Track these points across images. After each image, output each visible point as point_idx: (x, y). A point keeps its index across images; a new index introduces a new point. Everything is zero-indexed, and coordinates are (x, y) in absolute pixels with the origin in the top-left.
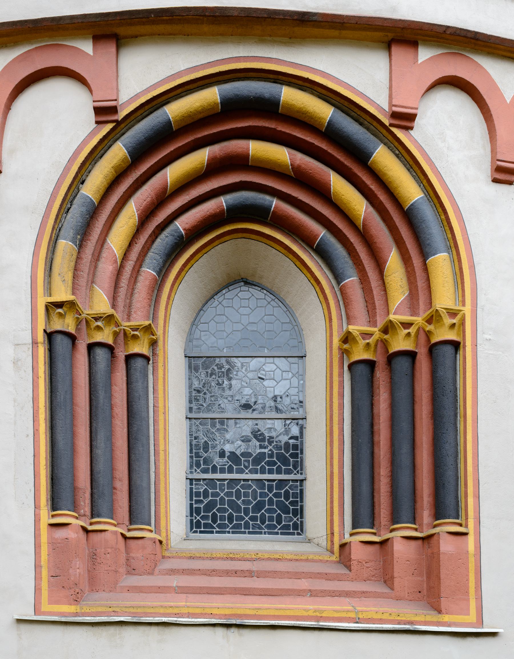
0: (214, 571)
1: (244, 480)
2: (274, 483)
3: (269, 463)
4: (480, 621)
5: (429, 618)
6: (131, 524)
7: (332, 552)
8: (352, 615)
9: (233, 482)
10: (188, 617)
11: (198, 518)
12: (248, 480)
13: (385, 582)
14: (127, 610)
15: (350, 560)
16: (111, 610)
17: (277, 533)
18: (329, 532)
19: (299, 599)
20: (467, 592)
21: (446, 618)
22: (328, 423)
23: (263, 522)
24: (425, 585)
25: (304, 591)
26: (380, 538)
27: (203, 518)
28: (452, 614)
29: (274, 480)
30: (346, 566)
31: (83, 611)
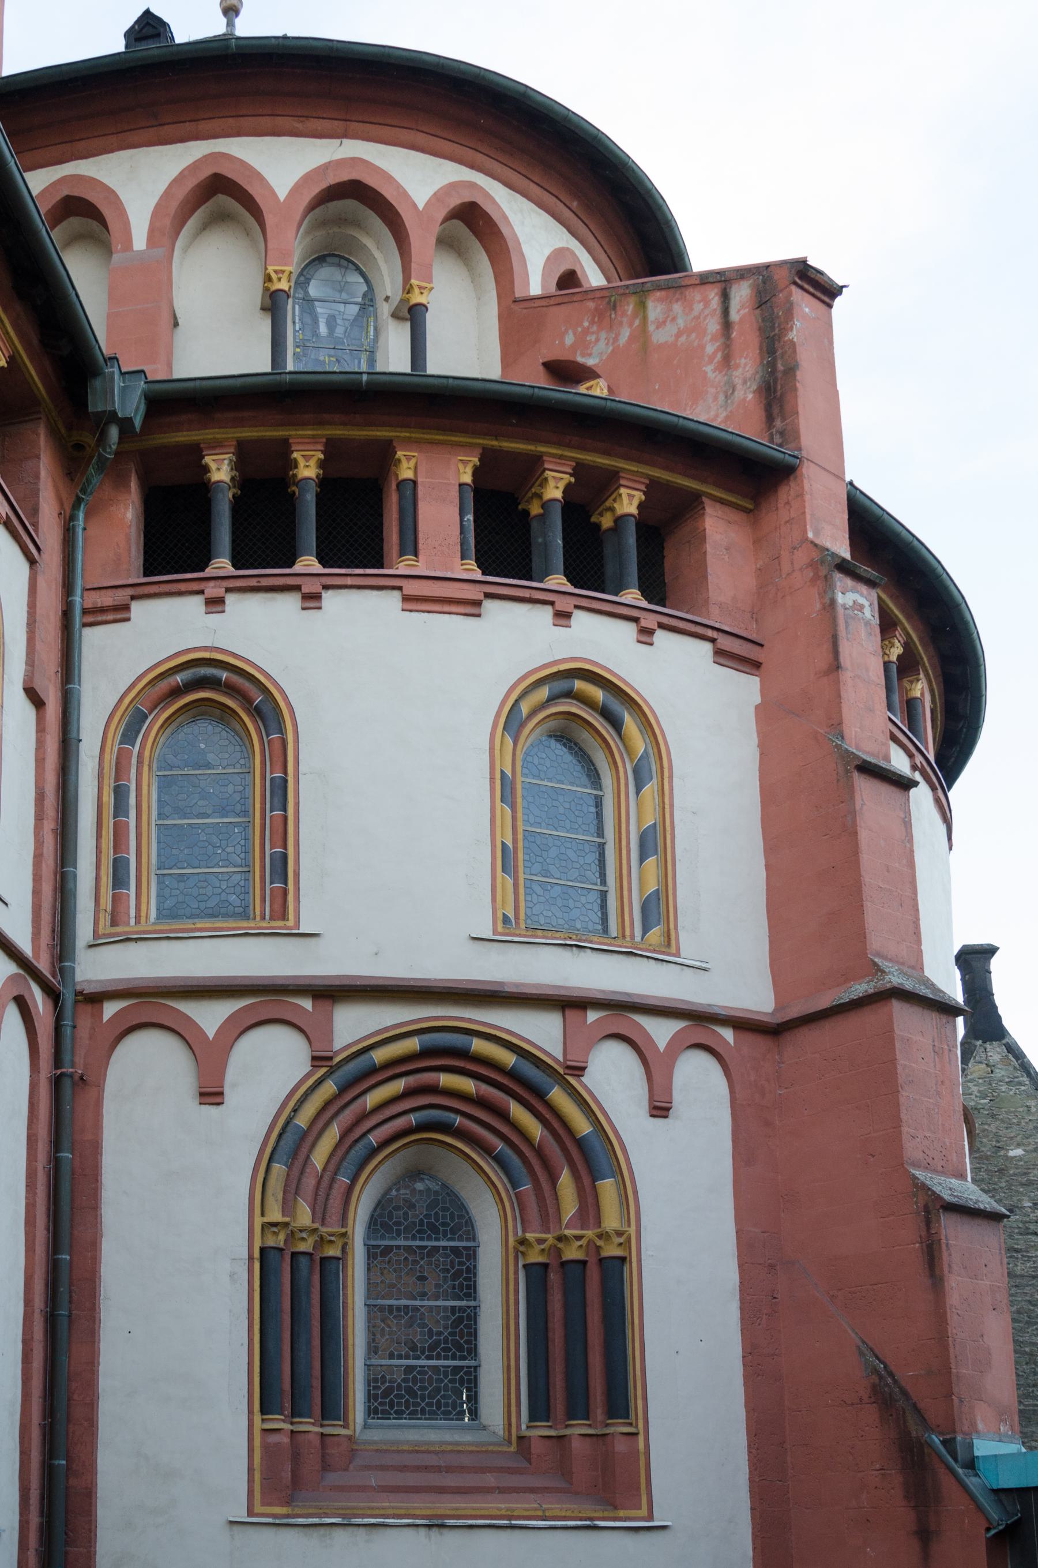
0: (405, 1466)
1: (420, 1366)
2: (449, 1369)
3: (444, 1350)
4: (650, 1517)
5: (606, 1514)
6: (323, 1419)
7: (510, 1442)
8: (540, 1513)
10: (393, 1518)
11: (376, 1404)
12: (424, 1367)
13: (563, 1475)
14: (337, 1512)
15: (530, 1453)
16: (321, 1511)
17: (452, 1419)
18: (506, 1423)
20: (639, 1488)
21: (621, 1513)
22: (505, 1317)
23: (439, 1407)
24: (600, 1479)
26: (557, 1432)
27: (381, 1404)
28: (626, 1509)
30: (525, 1458)
31: (294, 1512)
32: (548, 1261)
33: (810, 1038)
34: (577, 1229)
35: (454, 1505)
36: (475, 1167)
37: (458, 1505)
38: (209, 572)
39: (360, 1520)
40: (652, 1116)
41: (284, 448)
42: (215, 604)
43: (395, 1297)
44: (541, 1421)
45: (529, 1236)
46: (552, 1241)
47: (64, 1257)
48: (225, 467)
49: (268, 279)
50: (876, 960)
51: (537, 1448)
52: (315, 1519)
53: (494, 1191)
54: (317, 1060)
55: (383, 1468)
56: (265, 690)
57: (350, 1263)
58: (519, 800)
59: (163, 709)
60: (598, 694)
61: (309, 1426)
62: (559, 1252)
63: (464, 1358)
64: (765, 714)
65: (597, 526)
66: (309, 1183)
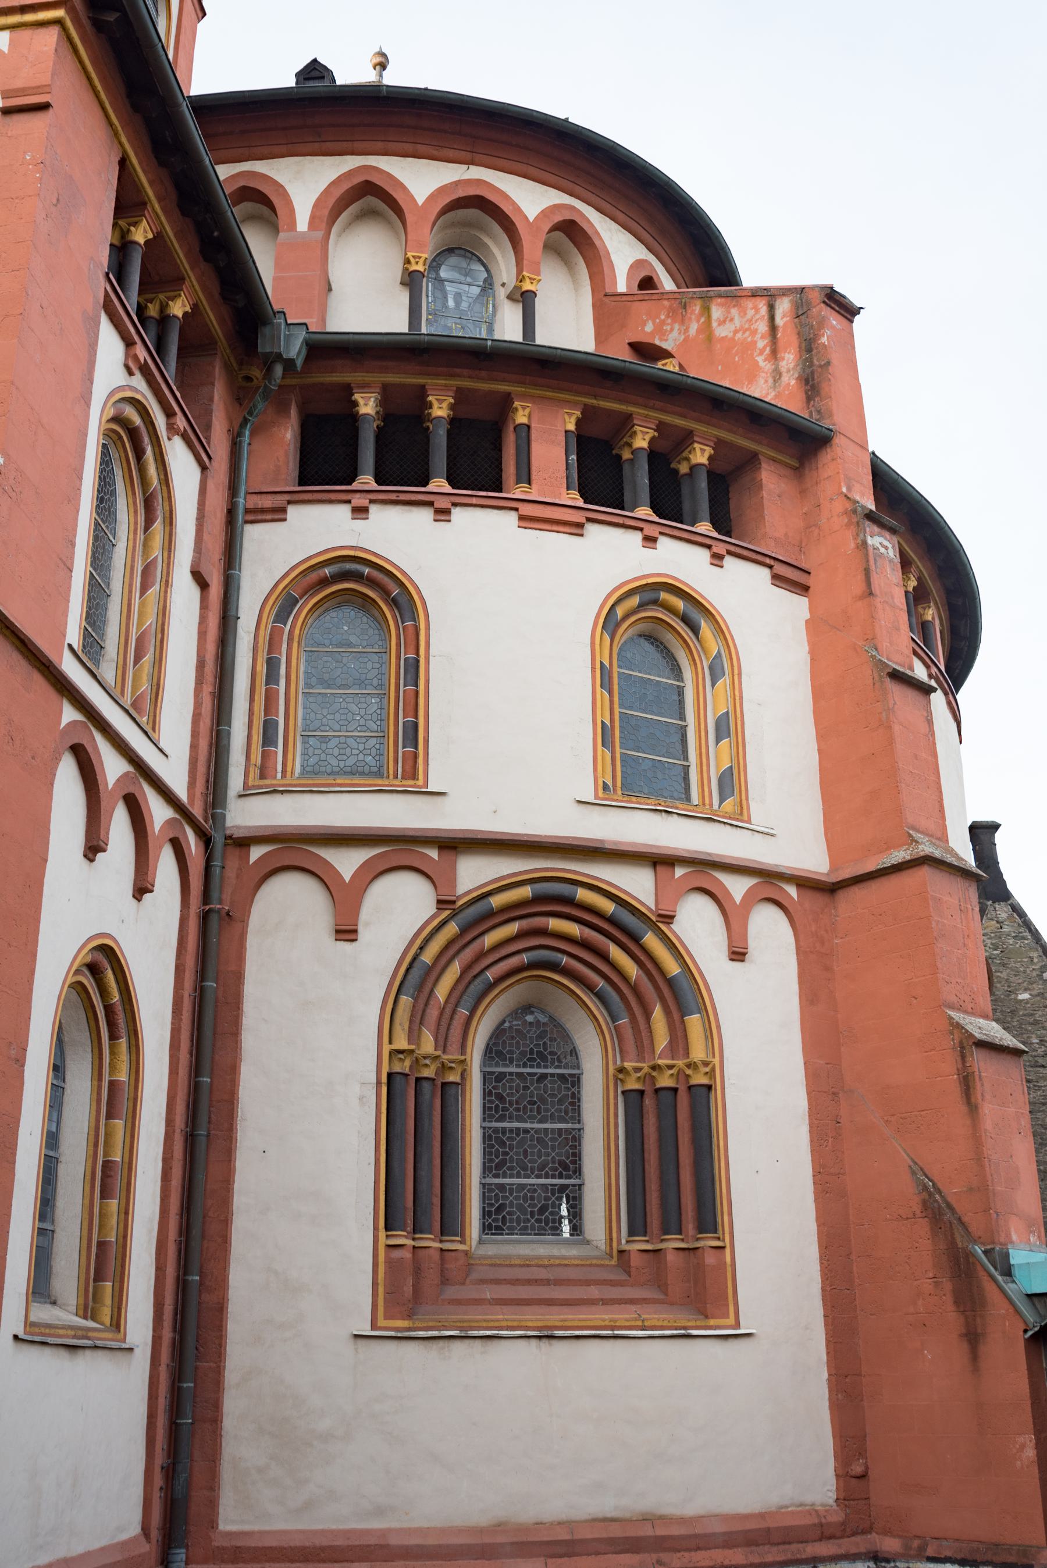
0: (517, 1280)
1: (530, 1185)
2: (557, 1188)
3: (552, 1169)
4: (737, 1325)
5: (699, 1323)
6: (442, 1235)
7: (611, 1256)
8: (639, 1323)
9: (522, 1187)
10: (507, 1330)
12: (534, 1185)
13: (659, 1287)
14: (454, 1324)
15: (630, 1266)
16: (440, 1324)
18: (608, 1238)
19: (594, 1308)
21: (712, 1322)
24: (692, 1291)
25: (596, 1300)
26: (653, 1246)
28: (716, 1318)
29: (556, 1185)
30: (625, 1271)
31: (415, 1325)
32: (644, 1088)
33: (857, 893)
34: (669, 1059)
35: (562, 1317)
36: (580, 1002)
37: (566, 1316)
38: (355, 486)
39: (476, 1332)
40: (732, 960)
41: (421, 393)
42: (360, 512)
43: (508, 1120)
44: (638, 1236)
45: (627, 1064)
46: (646, 1070)
47: (205, 1079)
48: (372, 403)
49: (407, 261)
50: (911, 832)
51: (636, 1261)
52: (434, 1332)
53: (596, 1023)
54: (442, 903)
55: (497, 1282)
56: (401, 584)
57: (468, 1088)
58: (616, 687)
59: (312, 596)
60: (680, 604)
61: (430, 1242)
62: (653, 1079)
63: (569, 1177)
64: (813, 626)
65: (676, 472)
66: (433, 1013)
